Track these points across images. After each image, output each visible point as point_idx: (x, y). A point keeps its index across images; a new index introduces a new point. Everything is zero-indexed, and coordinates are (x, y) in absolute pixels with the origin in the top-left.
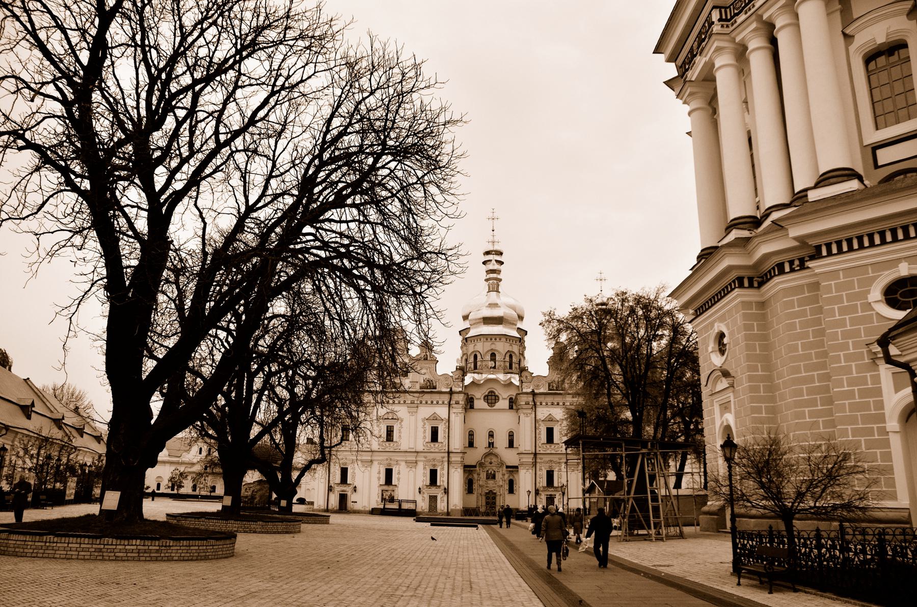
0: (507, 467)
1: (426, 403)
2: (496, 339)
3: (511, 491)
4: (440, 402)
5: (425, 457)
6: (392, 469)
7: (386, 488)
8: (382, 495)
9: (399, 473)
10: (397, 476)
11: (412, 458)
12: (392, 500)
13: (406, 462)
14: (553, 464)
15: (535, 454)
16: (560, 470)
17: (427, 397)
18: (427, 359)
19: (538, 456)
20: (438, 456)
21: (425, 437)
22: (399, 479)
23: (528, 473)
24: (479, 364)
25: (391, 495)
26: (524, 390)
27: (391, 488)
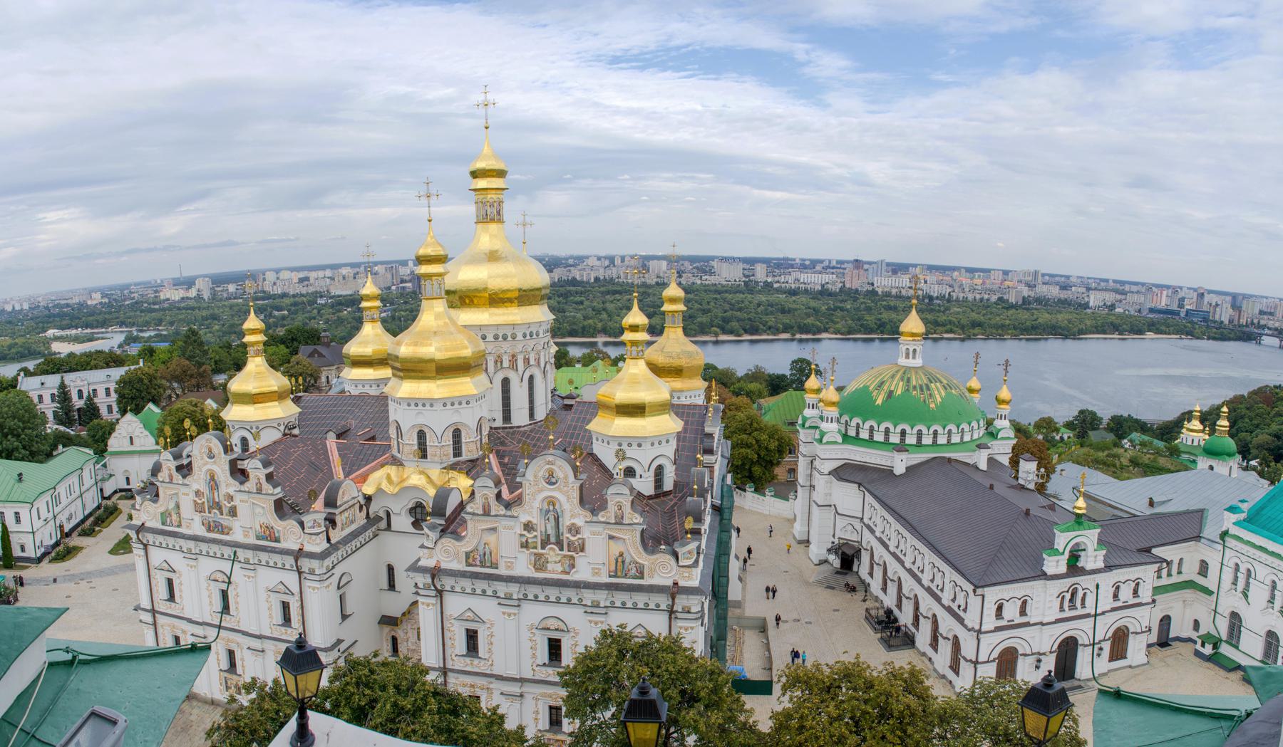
2: (424, 405)
24: (401, 446)
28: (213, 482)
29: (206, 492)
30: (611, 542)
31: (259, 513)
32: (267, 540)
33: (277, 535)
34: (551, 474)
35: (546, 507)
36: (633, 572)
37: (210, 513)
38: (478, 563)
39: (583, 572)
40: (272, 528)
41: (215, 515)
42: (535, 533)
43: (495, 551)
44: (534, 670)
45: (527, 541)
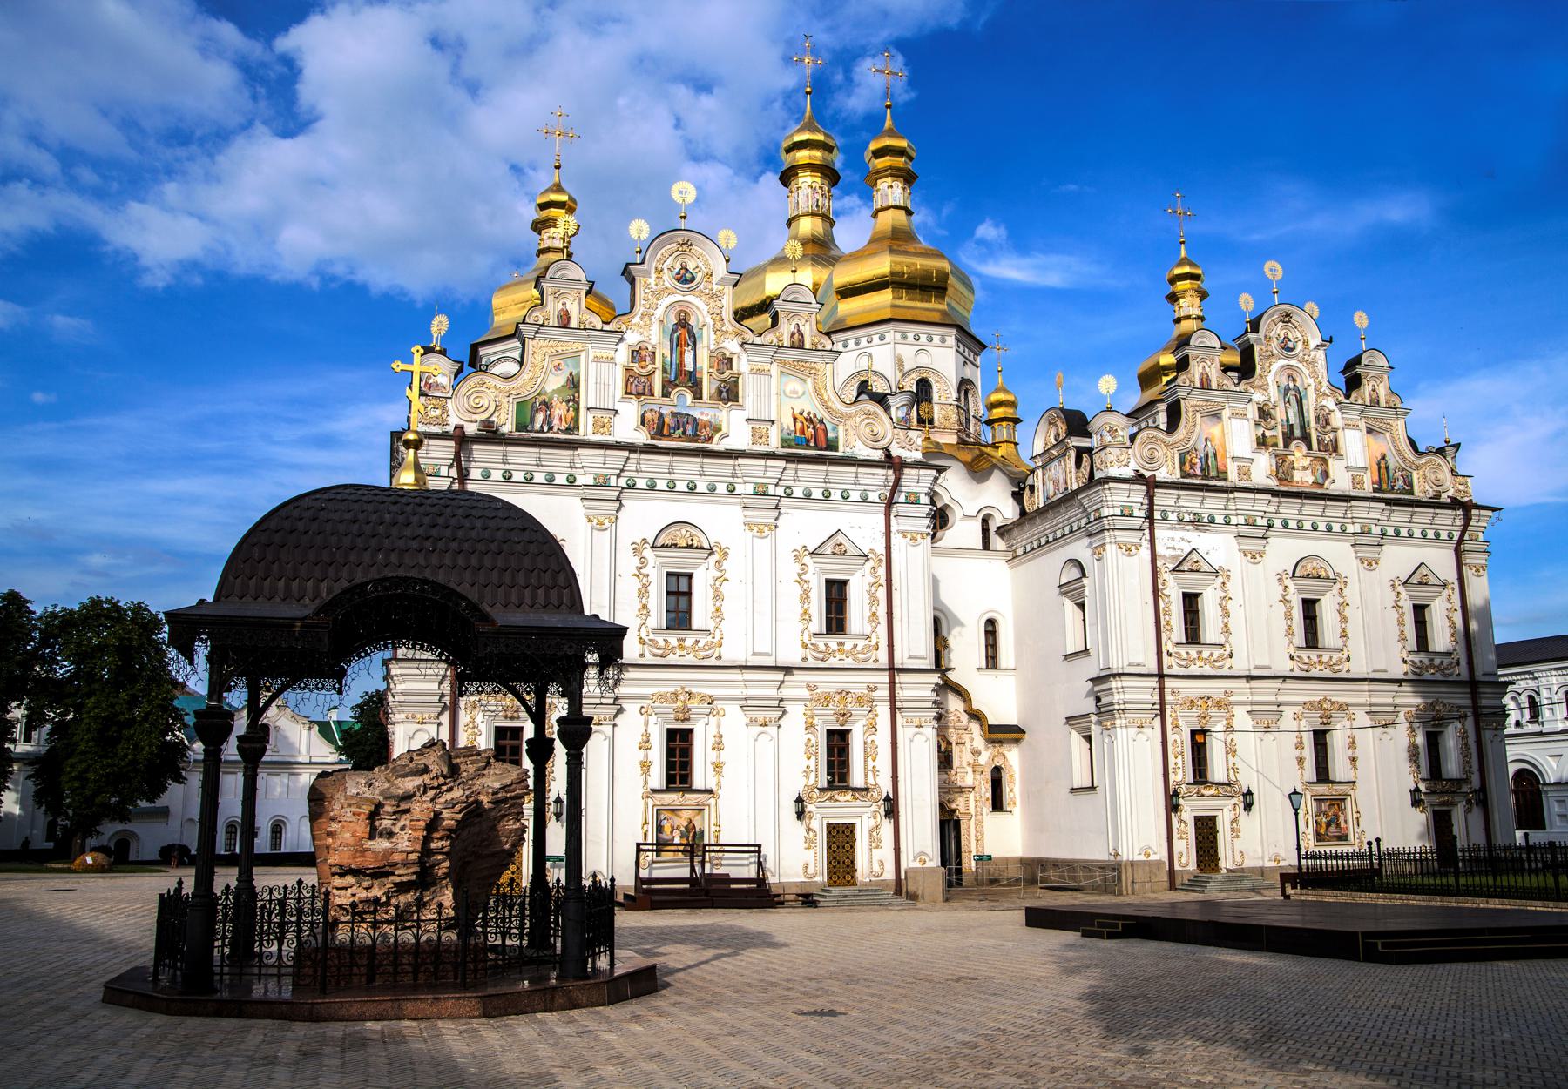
0: (994, 729)
1: (808, 496)
2: (930, 339)
3: (997, 804)
4: (855, 496)
5: (811, 687)
6: (687, 734)
7: (672, 799)
8: (660, 829)
9: (718, 746)
10: (712, 756)
11: (764, 687)
12: (694, 846)
13: (746, 704)
14: (1213, 711)
15: (1161, 676)
16: (1229, 729)
17: (812, 474)
18: (801, 347)
19: (1170, 684)
20: (857, 683)
21: (806, 616)
22: (718, 767)
23: (1142, 738)
25: (690, 826)
26: (1114, 471)
27: (691, 799)
28: (683, 332)
29: (664, 350)
30: (1370, 437)
31: (795, 392)
32: (808, 446)
33: (831, 435)
34: (1287, 337)
35: (1284, 382)
36: (1401, 482)
37: (666, 394)
38: (1198, 472)
39: (1340, 481)
40: (821, 421)
41: (683, 400)
42: (1273, 423)
43: (1221, 450)
44: (1292, 658)
45: (1263, 434)
